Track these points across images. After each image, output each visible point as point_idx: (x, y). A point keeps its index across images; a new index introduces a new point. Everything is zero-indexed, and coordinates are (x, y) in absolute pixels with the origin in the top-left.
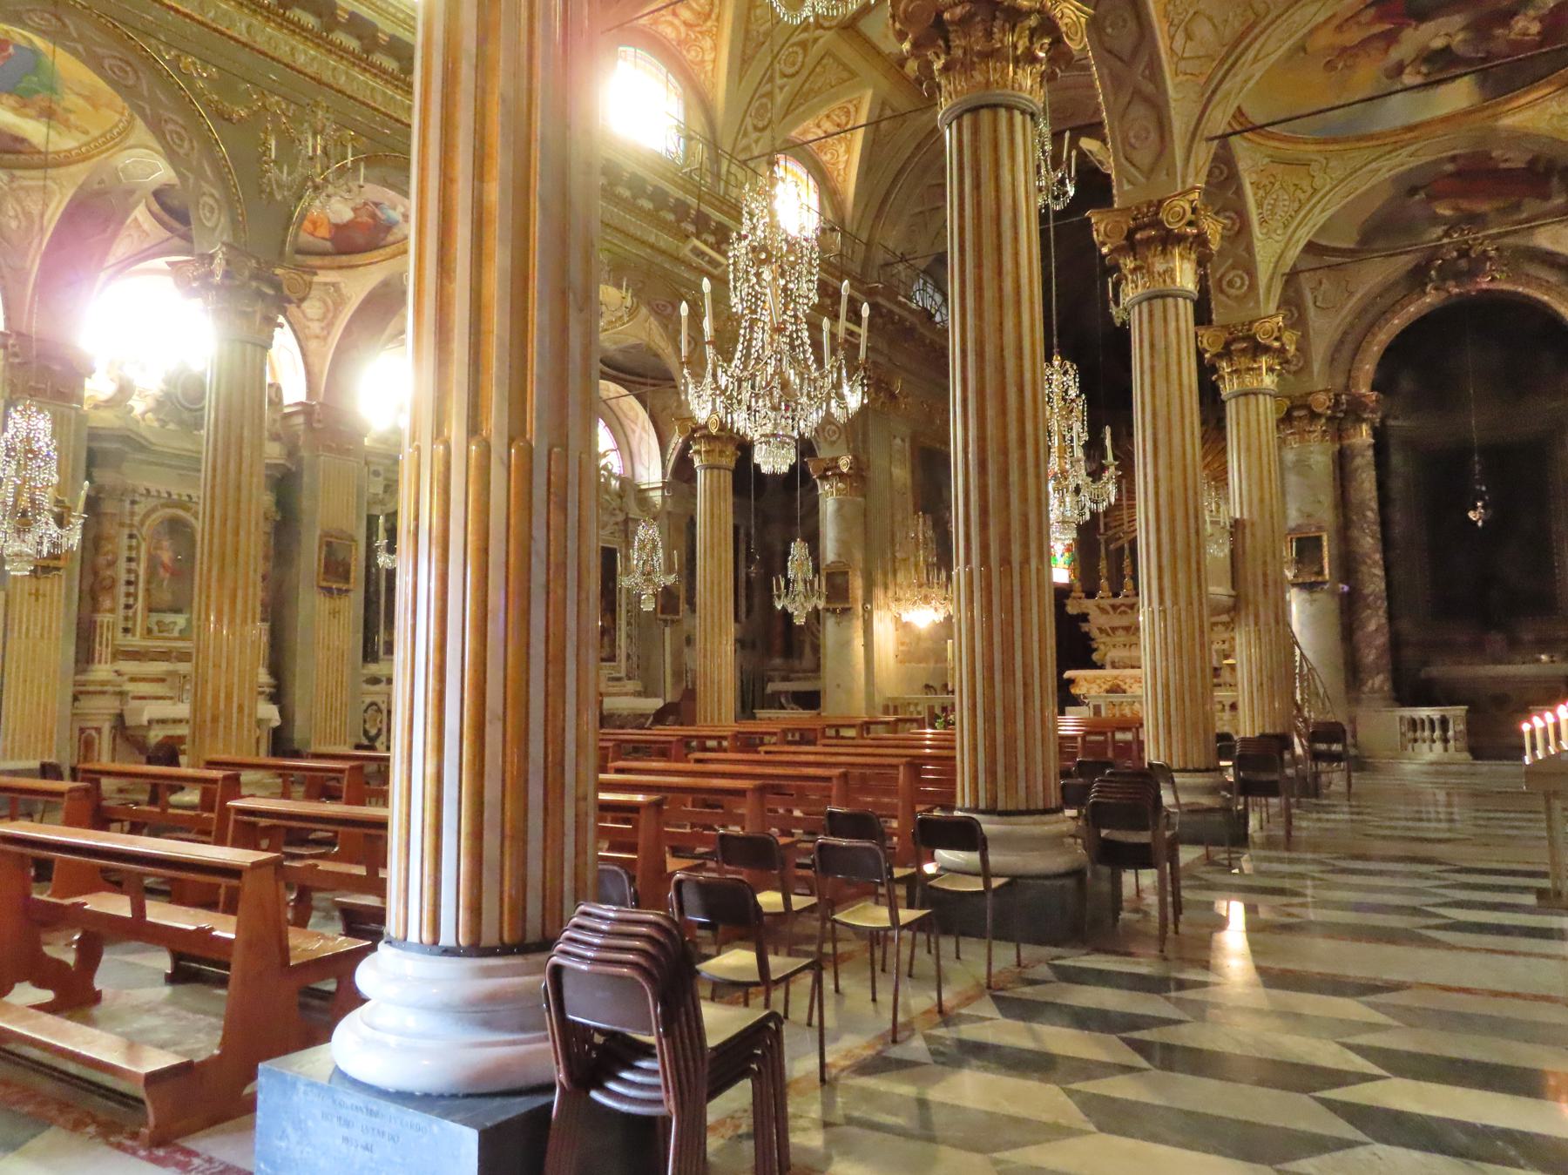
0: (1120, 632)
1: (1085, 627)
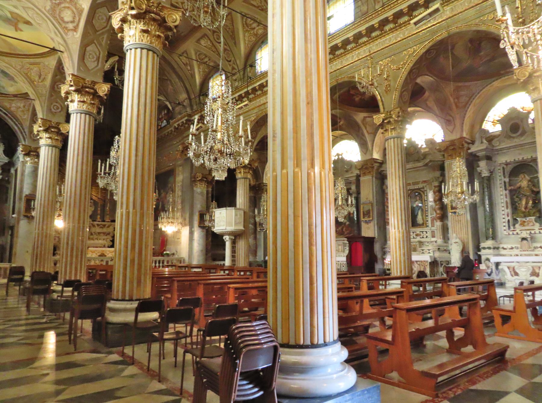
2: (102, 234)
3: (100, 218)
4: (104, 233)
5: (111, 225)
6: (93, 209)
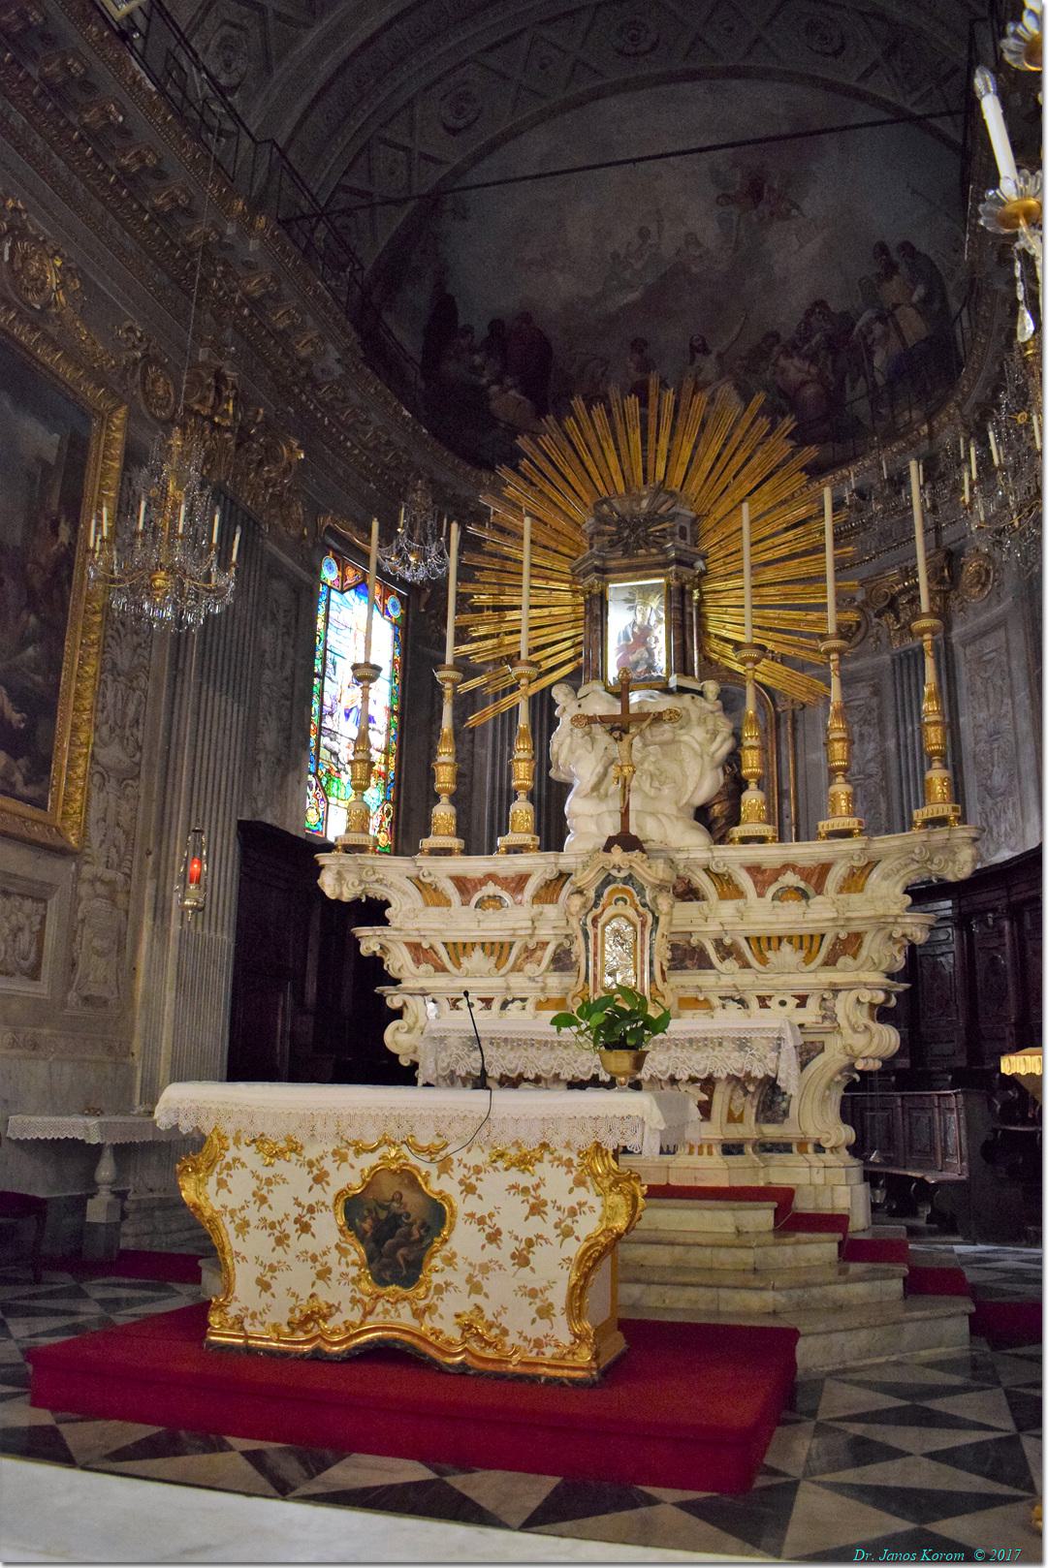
0: (477, 960)
1: (370, 940)
2: (788, 954)
3: (775, 815)
4: (807, 943)
5: (871, 865)
6: (722, 747)
